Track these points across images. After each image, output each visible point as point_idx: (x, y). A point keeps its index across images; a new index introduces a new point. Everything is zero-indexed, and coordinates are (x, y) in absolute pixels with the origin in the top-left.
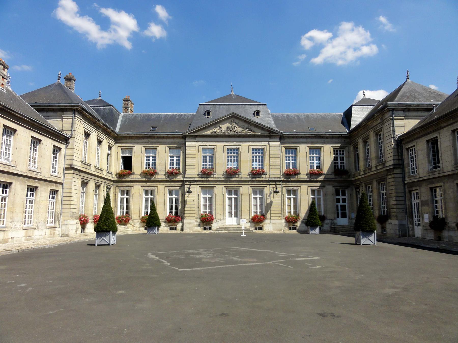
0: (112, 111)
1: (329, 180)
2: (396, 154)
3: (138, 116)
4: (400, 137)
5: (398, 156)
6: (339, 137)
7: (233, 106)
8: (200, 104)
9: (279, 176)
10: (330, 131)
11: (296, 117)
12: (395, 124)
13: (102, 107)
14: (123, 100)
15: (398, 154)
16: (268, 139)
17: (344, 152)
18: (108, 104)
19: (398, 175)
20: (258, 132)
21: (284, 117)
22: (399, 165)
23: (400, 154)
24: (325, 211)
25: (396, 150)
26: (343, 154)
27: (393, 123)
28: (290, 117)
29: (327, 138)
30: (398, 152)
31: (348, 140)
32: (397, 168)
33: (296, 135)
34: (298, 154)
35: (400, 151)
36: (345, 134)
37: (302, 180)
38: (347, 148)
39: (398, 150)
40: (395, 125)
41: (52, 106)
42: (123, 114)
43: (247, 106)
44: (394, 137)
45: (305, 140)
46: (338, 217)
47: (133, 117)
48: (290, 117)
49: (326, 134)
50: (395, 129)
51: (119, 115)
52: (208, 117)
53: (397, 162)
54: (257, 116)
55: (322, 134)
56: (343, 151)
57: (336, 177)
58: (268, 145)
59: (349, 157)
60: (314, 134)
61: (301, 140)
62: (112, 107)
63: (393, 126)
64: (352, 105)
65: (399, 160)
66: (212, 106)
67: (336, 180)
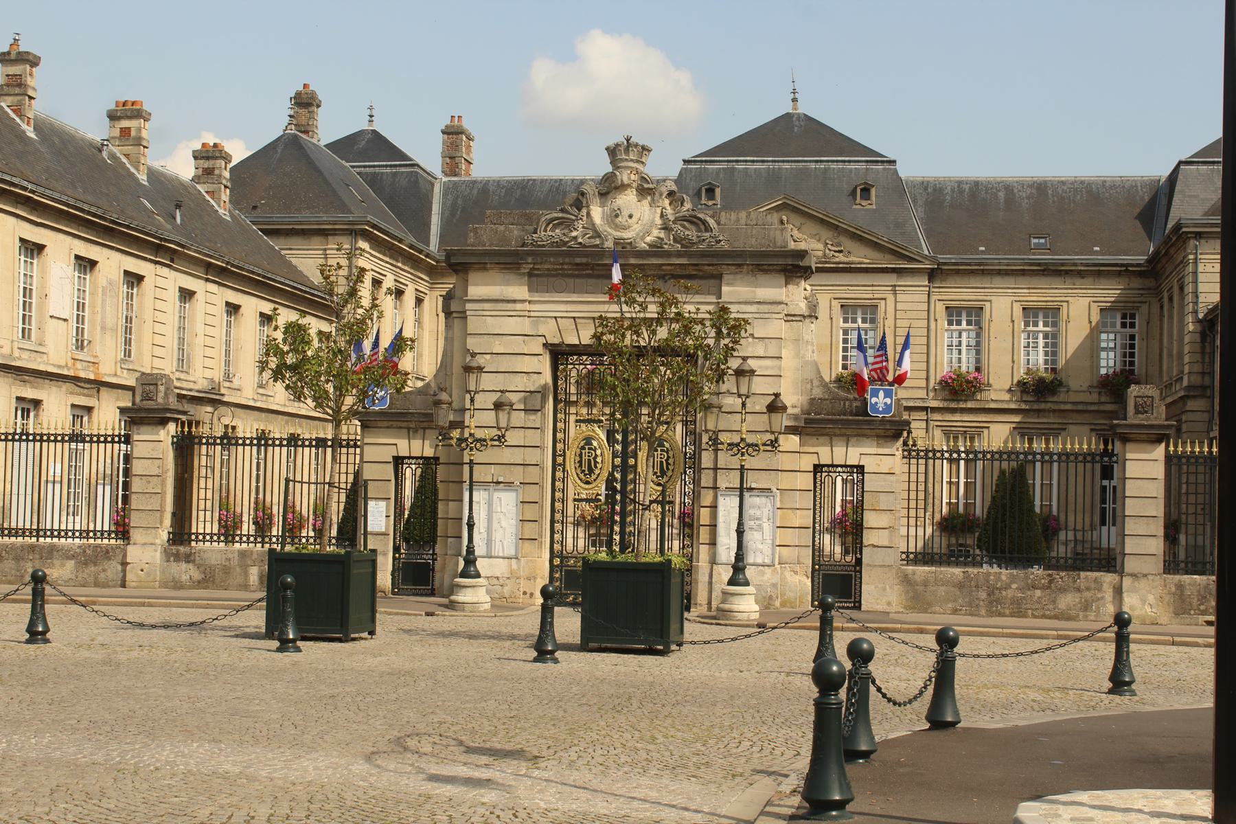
0: (416, 182)
1: (1080, 407)
2: (1198, 357)
3: (491, 188)
4: (1211, 311)
5: (1203, 363)
6: (1119, 274)
7: (787, 166)
8: (685, 161)
9: (922, 394)
10: (1098, 255)
11: (1001, 194)
12: (1200, 275)
13: (388, 170)
14: (443, 132)
15: (1203, 358)
16: (891, 279)
17: (1137, 321)
18: (403, 156)
19: (1198, 416)
20: (860, 256)
21: (961, 191)
22: (1204, 387)
23: (1207, 360)
24: (1064, 503)
25: (1197, 347)
26: (1132, 325)
27: (1195, 273)
28: (983, 194)
29: (1081, 274)
30: (1203, 353)
31: (1150, 283)
32: (1194, 397)
33: (980, 264)
34: (985, 324)
35: (1208, 350)
36: (1138, 265)
37: (993, 406)
38: (1145, 308)
39: (1203, 347)
40: (1201, 277)
41: (301, 223)
42: (445, 179)
43: (834, 166)
44: (1195, 312)
45: (1009, 281)
46: (1103, 523)
47: (475, 192)
48: (983, 194)
49: (1075, 265)
50: (1200, 290)
51: (433, 185)
52: (710, 203)
53: (1197, 380)
54: (864, 203)
55: (1062, 265)
56: (1133, 316)
57: (1103, 399)
58: (890, 298)
59: (1147, 337)
60: (1039, 265)
61: (998, 281)
62: (416, 169)
63: (1195, 282)
64: (1180, 163)
65: (1203, 374)
66: (724, 166)
67: (1102, 408)
